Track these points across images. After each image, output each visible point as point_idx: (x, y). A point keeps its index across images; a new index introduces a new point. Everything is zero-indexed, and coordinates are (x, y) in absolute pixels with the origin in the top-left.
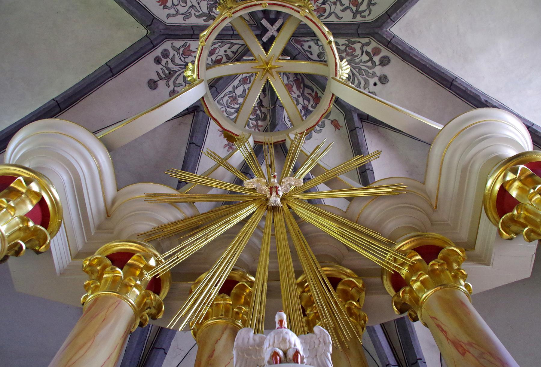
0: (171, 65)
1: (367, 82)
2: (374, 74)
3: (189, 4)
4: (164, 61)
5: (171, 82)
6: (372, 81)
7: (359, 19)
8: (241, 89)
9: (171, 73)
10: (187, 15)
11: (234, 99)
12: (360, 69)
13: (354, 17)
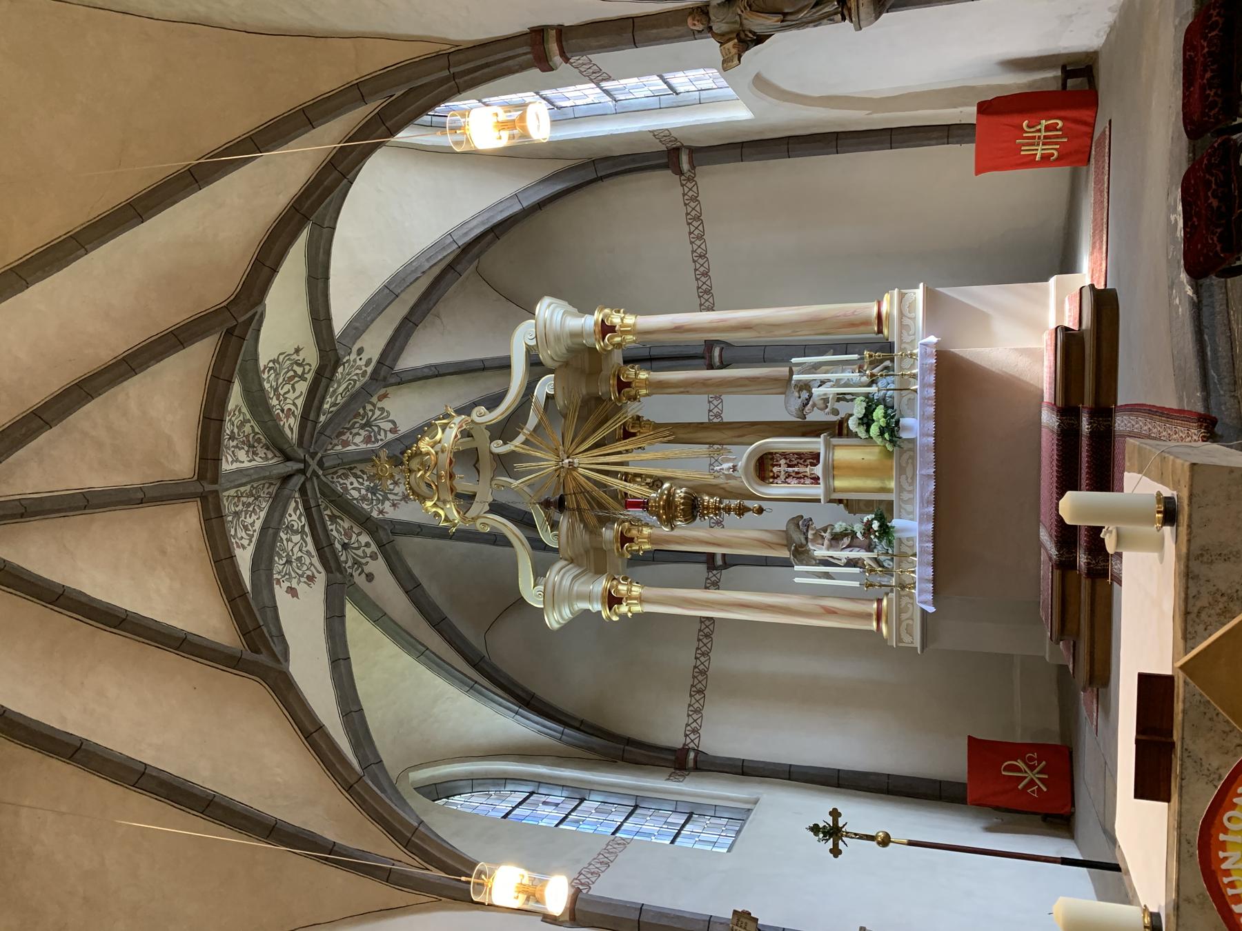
0: (349, 564)
1: (359, 368)
2: (355, 361)
3: (300, 554)
4: (349, 571)
5: (364, 561)
6: (359, 363)
7: (309, 376)
8: (353, 492)
9: (356, 562)
10: (308, 553)
11: (364, 498)
12: (348, 374)
13: (305, 380)
